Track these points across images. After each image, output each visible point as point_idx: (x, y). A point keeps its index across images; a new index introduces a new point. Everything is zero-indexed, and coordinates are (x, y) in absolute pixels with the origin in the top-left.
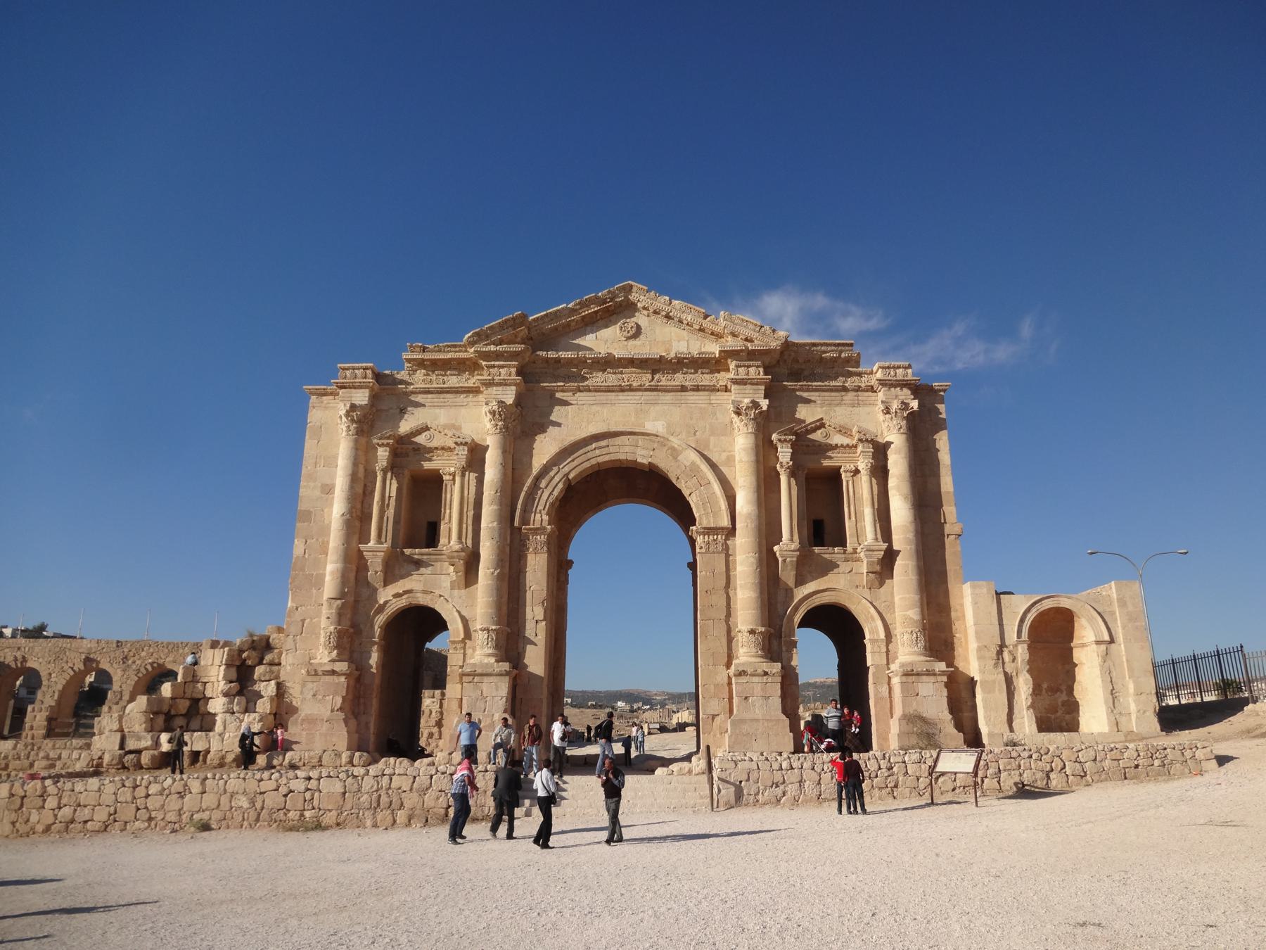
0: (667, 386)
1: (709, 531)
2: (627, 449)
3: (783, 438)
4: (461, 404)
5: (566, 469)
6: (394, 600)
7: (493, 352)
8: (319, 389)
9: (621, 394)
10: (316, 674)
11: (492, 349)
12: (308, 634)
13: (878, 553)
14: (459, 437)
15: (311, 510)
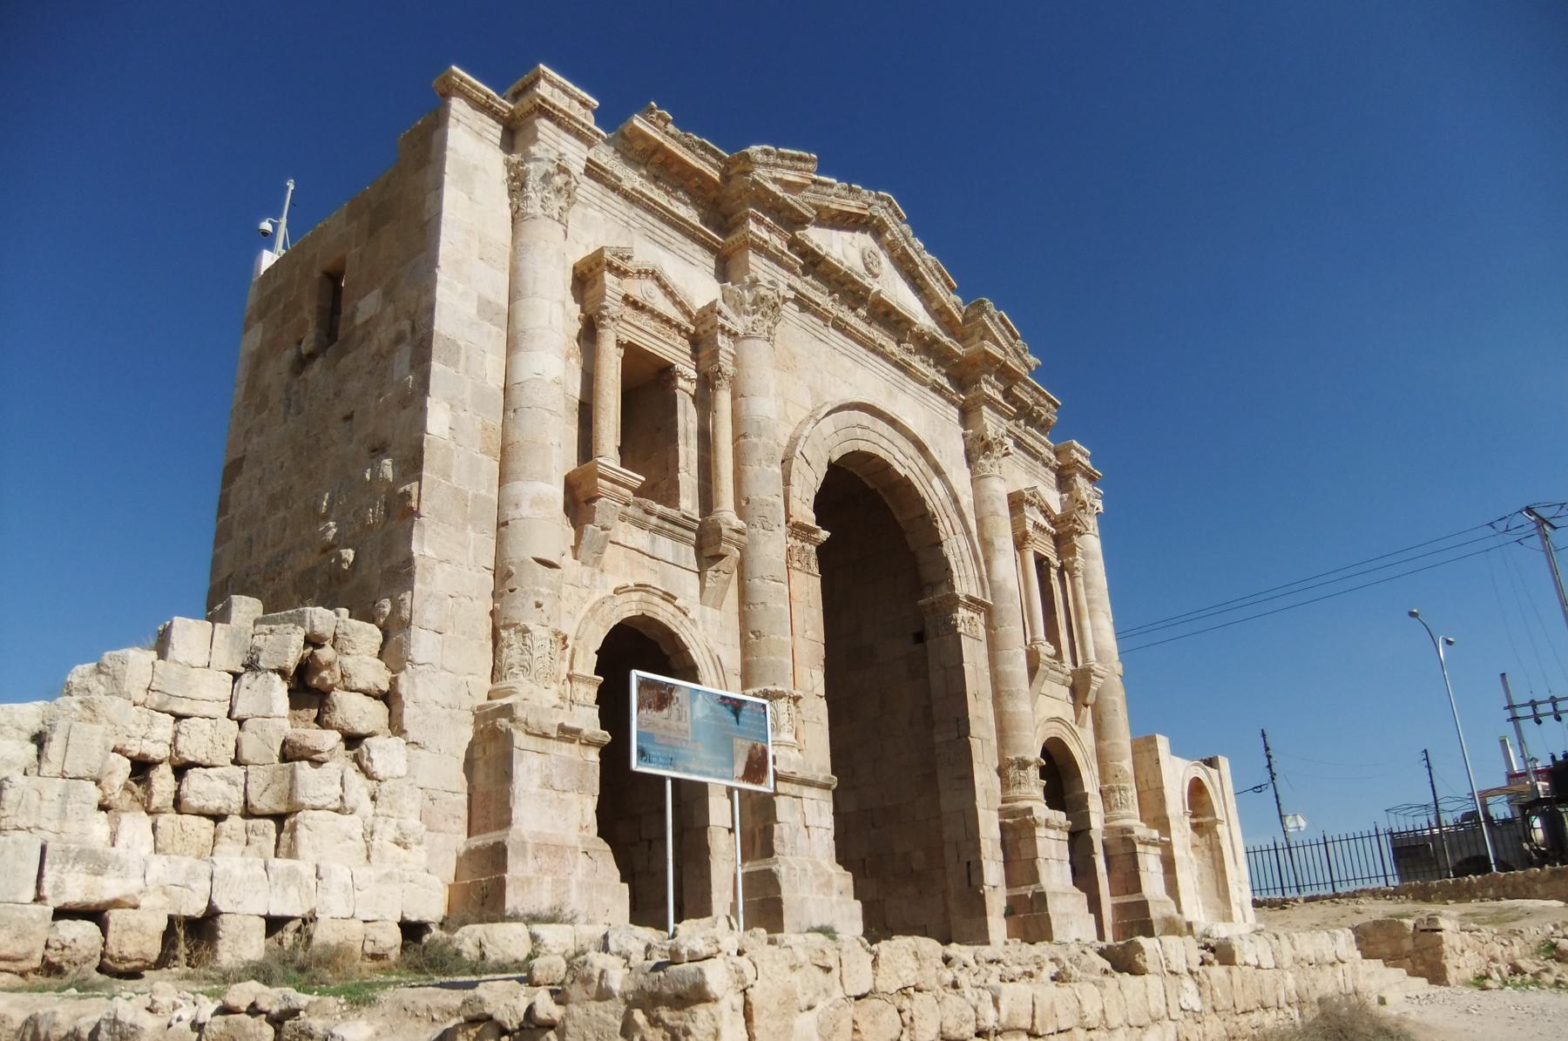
0: (918, 370)
1: (973, 603)
2: (885, 443)
3: (1031, 498)
4: (692, 260)
5: (829, 443)
6: (620, 599)
7: (779, 198)
8: (479, 90)
9: (871, 355)
10: (545, 736)
11: (778, 193)
12: (464, 633)
13: (1099, 680)
14: (726, 318)
15: (462, 343)
